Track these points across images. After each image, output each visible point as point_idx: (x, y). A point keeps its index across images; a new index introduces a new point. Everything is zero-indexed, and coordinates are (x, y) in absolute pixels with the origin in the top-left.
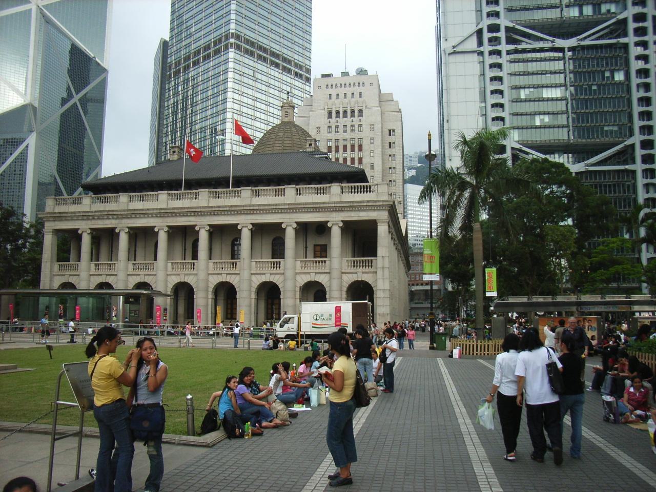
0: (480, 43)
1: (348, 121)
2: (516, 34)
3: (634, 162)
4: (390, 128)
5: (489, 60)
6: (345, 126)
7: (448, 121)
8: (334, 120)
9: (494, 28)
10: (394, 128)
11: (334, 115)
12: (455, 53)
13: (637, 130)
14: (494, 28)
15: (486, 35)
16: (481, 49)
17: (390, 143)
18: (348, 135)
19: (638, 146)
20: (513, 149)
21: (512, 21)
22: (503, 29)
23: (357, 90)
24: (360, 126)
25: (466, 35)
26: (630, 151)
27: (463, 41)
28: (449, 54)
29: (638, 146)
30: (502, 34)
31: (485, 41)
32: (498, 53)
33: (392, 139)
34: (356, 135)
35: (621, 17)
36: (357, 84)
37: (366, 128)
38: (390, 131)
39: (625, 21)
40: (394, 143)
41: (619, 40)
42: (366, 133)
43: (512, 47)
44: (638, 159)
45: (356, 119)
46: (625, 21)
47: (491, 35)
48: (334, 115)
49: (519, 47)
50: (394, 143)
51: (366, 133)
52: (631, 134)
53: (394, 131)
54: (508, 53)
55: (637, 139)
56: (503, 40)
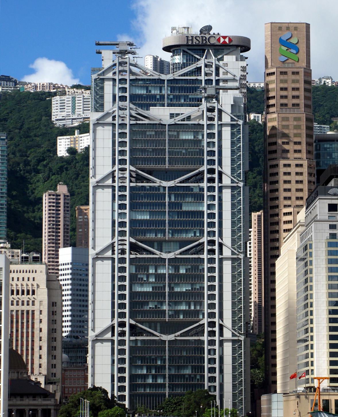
1: (25, 298)
4: (54, 301)
6: (23, 301)
8: (15, 296)
11: (15, 292)
17: (53, 312)
18: (25, 308)
23: (31, 275)
24: (33, 302)
34: (30, 308)
36: (31, 271)
37: (37, 303)
38: (53, 303)
42: (36, 308)
45: (30, 296)
48: (15, 292)
51: (36, 308)
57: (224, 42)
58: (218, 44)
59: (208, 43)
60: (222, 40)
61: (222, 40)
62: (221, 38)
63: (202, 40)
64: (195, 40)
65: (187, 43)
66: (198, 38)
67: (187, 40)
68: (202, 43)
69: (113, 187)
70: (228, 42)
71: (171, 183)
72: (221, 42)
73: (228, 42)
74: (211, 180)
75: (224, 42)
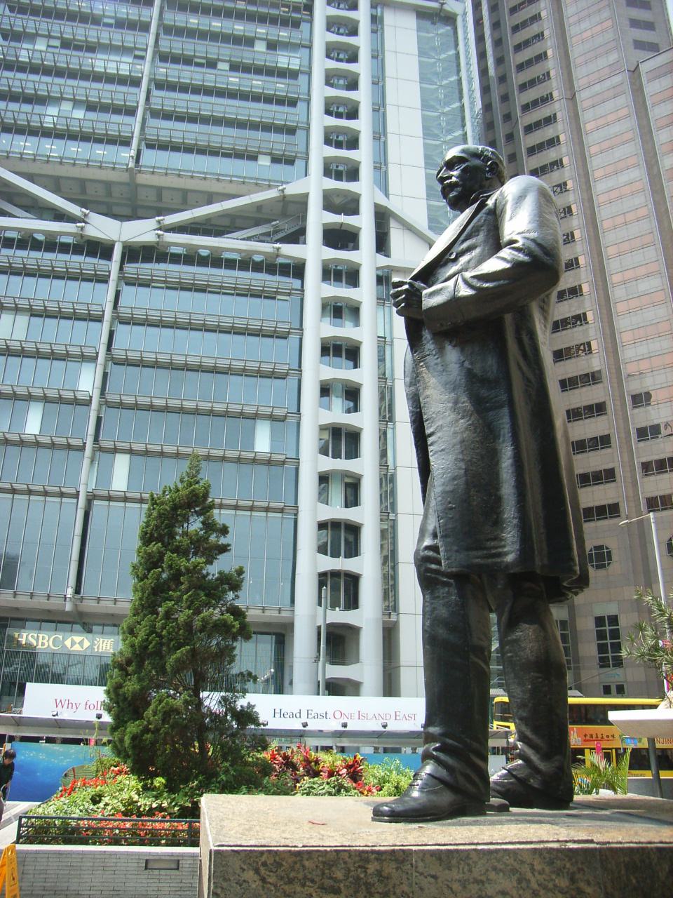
71: (142, 231)
74: (340, 238)
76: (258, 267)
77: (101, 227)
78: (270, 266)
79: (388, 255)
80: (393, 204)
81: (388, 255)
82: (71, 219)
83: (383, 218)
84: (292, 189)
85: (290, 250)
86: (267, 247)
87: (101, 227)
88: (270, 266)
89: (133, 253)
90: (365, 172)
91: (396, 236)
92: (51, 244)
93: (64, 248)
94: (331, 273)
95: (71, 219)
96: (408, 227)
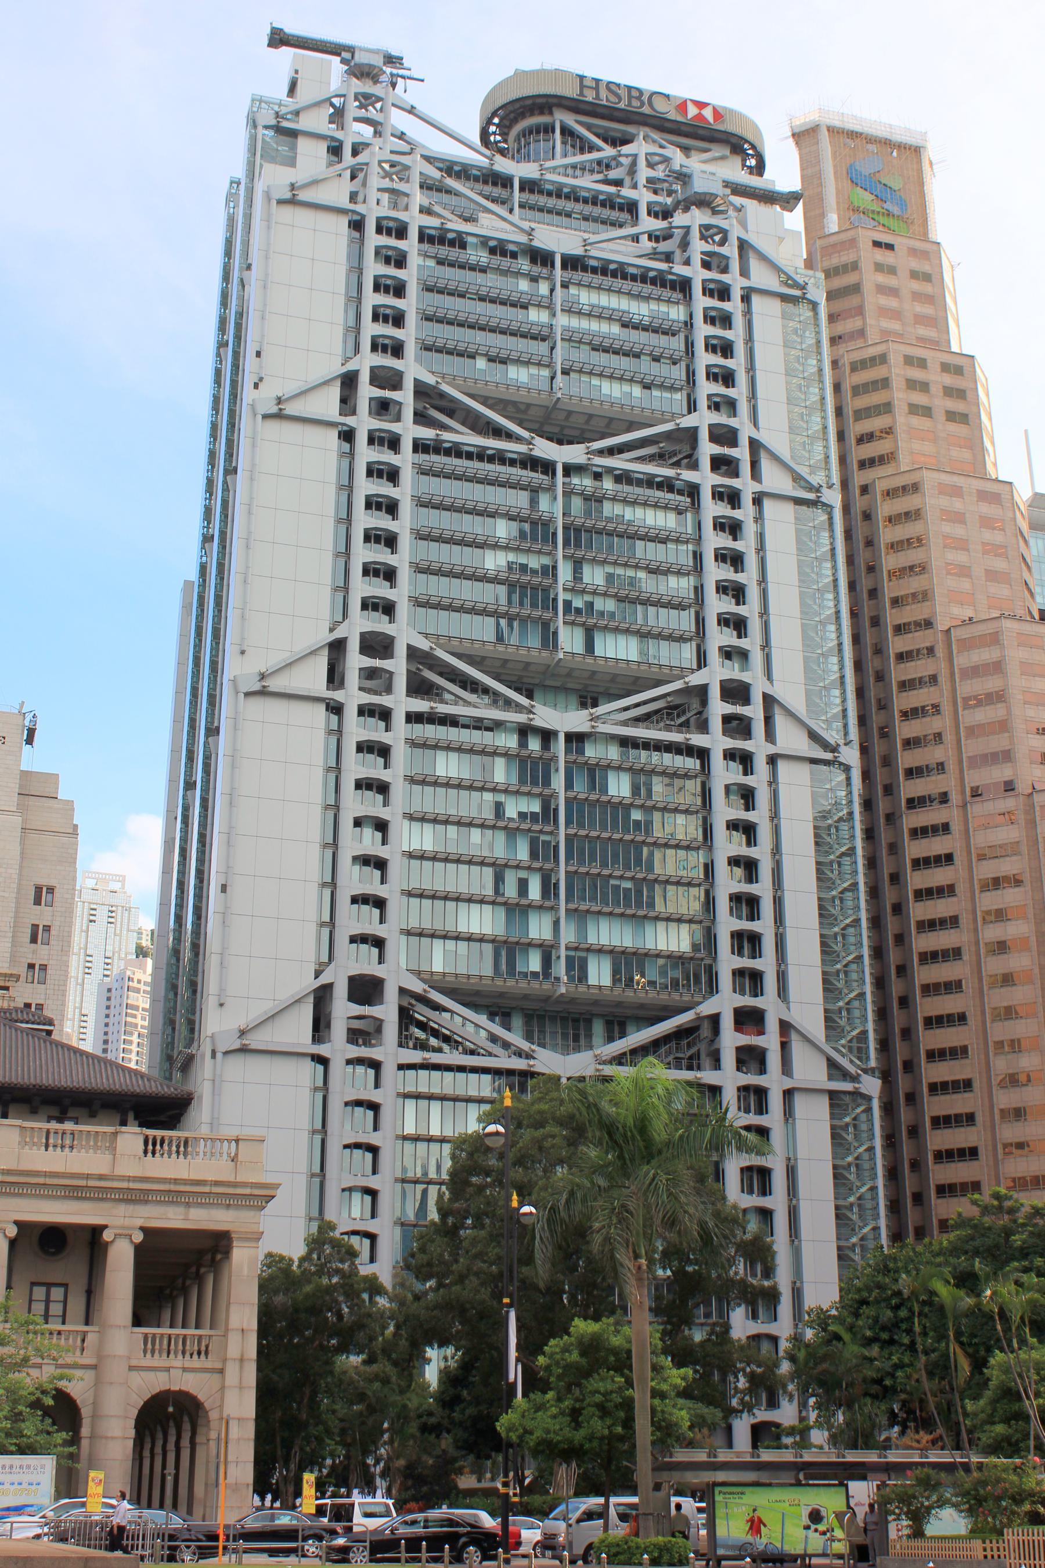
0: (335, 677)
2: (431, 668)
3: (717, 1065)
5: (357, 729)
7: (224, 888)
9: (377, 645)
10: (52, 883)
12: (263, 692)
13: (725, 980)
14: (377, 645)
15: (355, 661)
16: (338, 696)
17: (35, 927)
19: (727, 1022)
20: (402, 991)
21: (426, 635)
22: (401, 651)
25: (303, 645)
26: (705, 1032)
27: (290, 664)
28: (247, 694)
29: (727, 1022)
30: (398, 665)
31: (352, 678)
32: (385, 715)
33: (42, 915)
35: (696, 679)
38: (38, 890)
39: (702, 691)
40: (47, 928)
41: (688, 736)
43: (421, 705)
44: (728, 1058)
46: (702, 691)
47: (368, 662)
49: (442, 709)
50: (47, 928)
52: (713, 987)
53: (51, 890)
54: (413, 718)
55: (725, 1002)
56: (401, 683)
57: (700, 117)
58: (680, 119)
59: (646, 110)
60: (692, 111)
61: (692, 111)
62: (689, 103)
63: (630, 97)
64: (603, 93)
65: (581, 94)
66: (613, 87)
67: (582, 86)
68: (629, 105)
69: (348, 436)
70: (711, 120)
71: (574, 453)
72: (690, 115)
73: (711, 120)
75: (700, 117)
76: (660, 486)
77: (544, 449)
78: (667, 485)
79: (760, 481)
80: (762, 437)
81: (760, 481)
82: (519, 439)
83: (755, 446)
84: (688, 422)
85: (689, 476)
86: (670, 472)
87: (544, 449)
88: (667, 485)
89: (569, 470)
90: (743, 407)
91: (766, 465)
92: (499, 458)
93: (512, 463)
94: (718, 495)
95: (519, 439)
96: (775, 458)
